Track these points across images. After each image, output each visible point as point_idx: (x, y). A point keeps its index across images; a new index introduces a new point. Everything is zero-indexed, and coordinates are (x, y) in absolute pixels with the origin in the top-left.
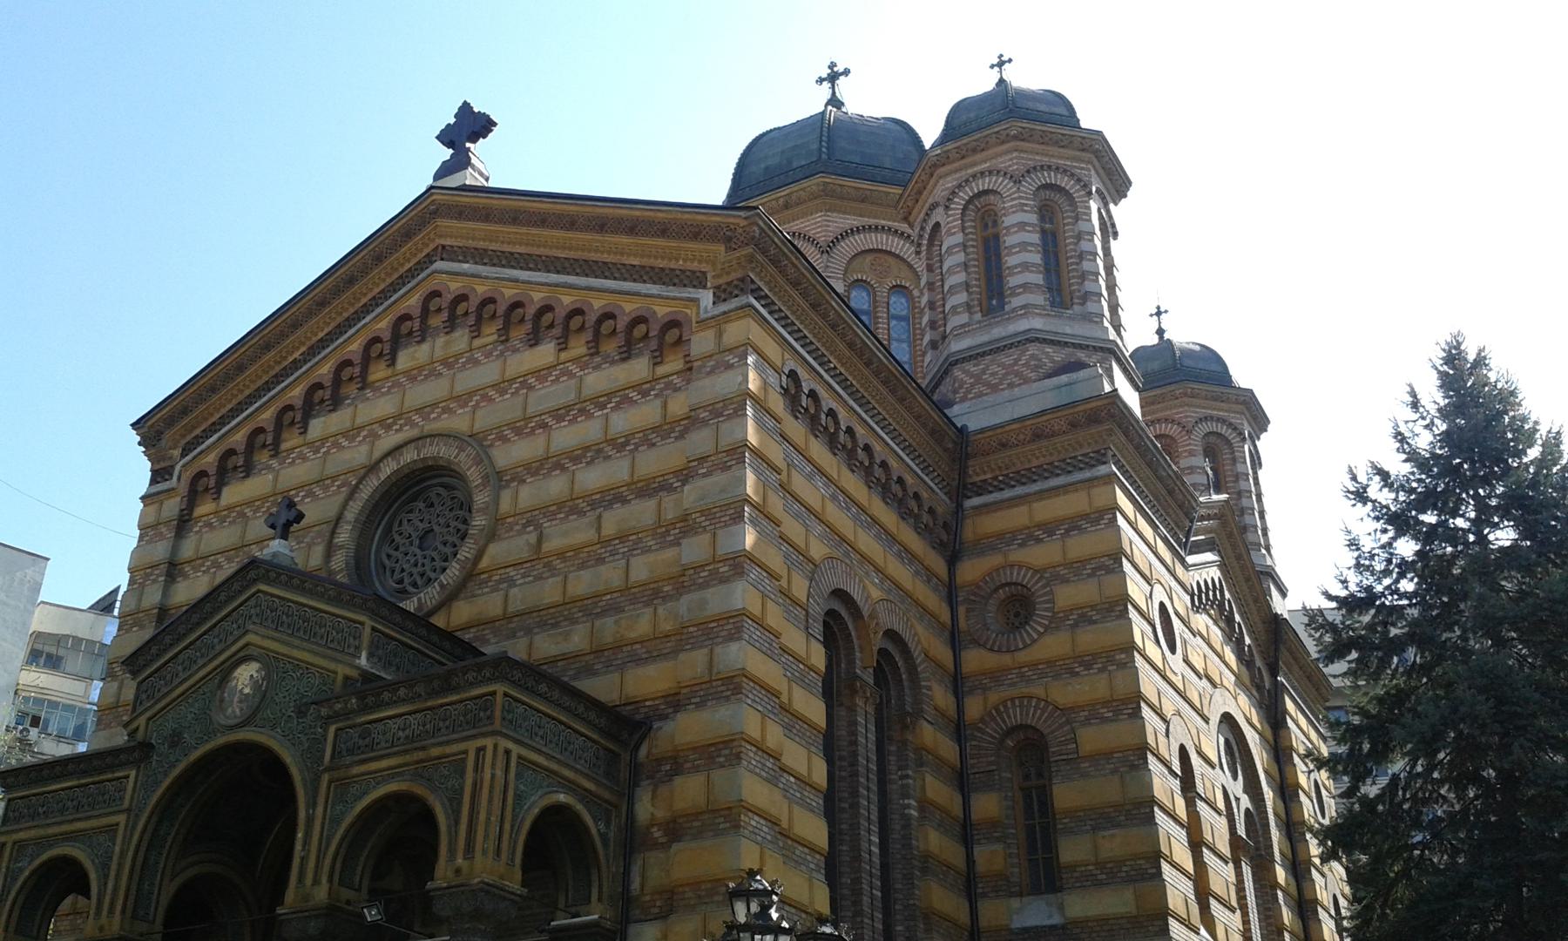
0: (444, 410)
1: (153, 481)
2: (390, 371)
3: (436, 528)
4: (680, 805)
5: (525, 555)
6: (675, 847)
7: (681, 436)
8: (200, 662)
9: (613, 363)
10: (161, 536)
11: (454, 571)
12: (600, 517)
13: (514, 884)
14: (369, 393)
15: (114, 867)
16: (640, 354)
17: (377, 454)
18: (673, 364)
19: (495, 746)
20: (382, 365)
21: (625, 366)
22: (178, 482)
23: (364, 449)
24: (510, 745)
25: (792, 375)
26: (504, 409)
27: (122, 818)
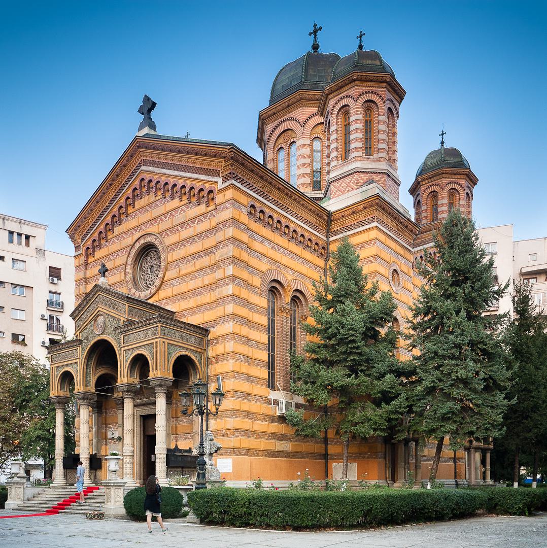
0: (151, 224)
1: (76, 251)
2: (134, 210)
3: (154, 265)
4: (218, 352)
5: (176, 275)
6: (217, 364)
7: (215, 234)
8: (89, 315)
9: (196, 206)
10: (81, 270)
11: (158, 282)
12: (195, 263)
13: (171, 377)
15: (79, 373)
16: (203, 203)
17: (134, 241)
18: (212, 207)
20: (131, 207)
22: (82, 251)
23: (130, 238)
24: (165, 340)
25: (253, 206)
26: (166, 224)
27: (78, 360)
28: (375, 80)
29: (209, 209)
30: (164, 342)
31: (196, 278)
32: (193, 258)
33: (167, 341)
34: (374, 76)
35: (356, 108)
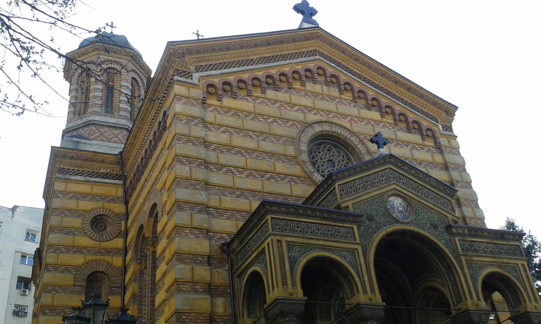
2: (303, 88)
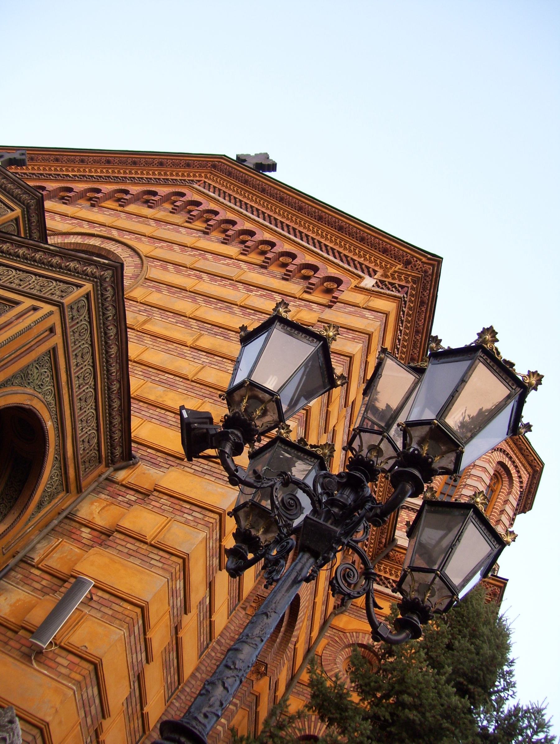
2: (120, 208)
4: (126, 524)
12: (201, 335)
14: (95, 209)
19: (51, 313)
21: (284, 282)
28: (526, 453)
29: (306, 296)
30: (52, 330)
31: (182, 356)
32: (201, 328)
33: (57, 339)
34: (527, 449)
35: (490, 457)
